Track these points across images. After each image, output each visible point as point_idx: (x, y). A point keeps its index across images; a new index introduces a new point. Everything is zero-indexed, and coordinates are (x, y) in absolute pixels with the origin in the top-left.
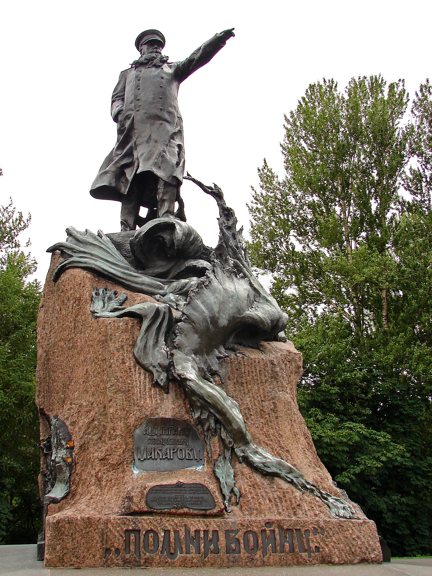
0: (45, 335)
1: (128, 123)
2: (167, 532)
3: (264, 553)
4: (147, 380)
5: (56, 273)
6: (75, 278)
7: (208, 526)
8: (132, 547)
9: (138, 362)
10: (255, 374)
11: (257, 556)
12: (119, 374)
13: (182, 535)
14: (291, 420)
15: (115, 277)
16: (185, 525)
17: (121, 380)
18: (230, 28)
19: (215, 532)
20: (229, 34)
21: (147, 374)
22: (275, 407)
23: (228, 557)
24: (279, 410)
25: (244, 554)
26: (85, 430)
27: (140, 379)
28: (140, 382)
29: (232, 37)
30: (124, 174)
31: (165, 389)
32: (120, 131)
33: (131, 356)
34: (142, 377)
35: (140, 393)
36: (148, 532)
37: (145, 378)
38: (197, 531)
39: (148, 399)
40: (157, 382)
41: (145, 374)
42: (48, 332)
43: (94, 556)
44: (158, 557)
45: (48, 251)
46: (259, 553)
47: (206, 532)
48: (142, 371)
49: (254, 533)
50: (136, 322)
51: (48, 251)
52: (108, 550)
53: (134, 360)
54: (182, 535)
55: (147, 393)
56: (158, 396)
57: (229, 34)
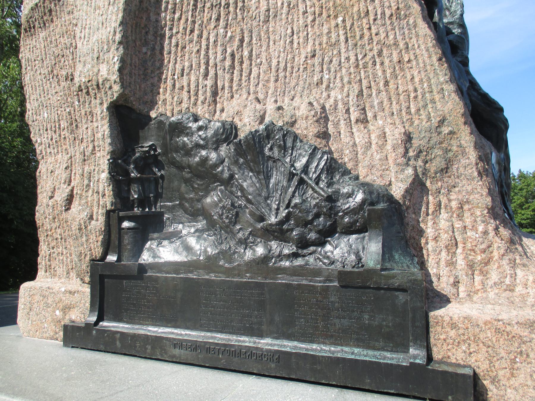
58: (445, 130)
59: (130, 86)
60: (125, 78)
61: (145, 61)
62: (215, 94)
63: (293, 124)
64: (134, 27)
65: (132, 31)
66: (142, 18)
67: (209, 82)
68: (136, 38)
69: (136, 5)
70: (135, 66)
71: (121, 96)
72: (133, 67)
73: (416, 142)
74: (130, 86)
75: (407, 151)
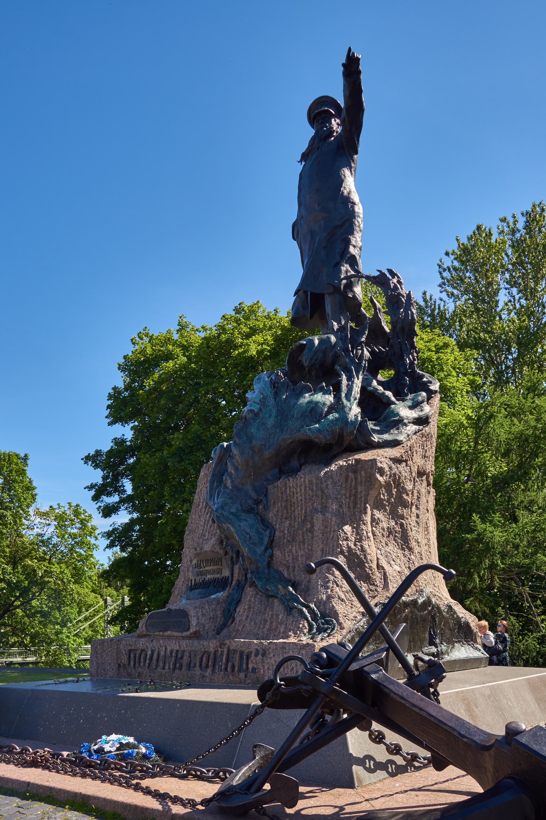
2: (153, 652)
3: (213, 671)
7: (180, 646)
8: (132, 663)
11: (207, 674)
13: (162, 653)
14: (328, 539)
16: (166, 646)
19: (184, 651)
22: (312, 526)
23: (187, 674)
24: (316, 528)
25: (197, 671)
28: (205, 520)
35: (203, 530)
36: (143, 651)
38: (171, 651)
43: (113, 669)
44: (145, 672)
46: (209, 671)
47: (177, 651)
49: (209, 654)
52: (119, 666)
54: (162, 653)
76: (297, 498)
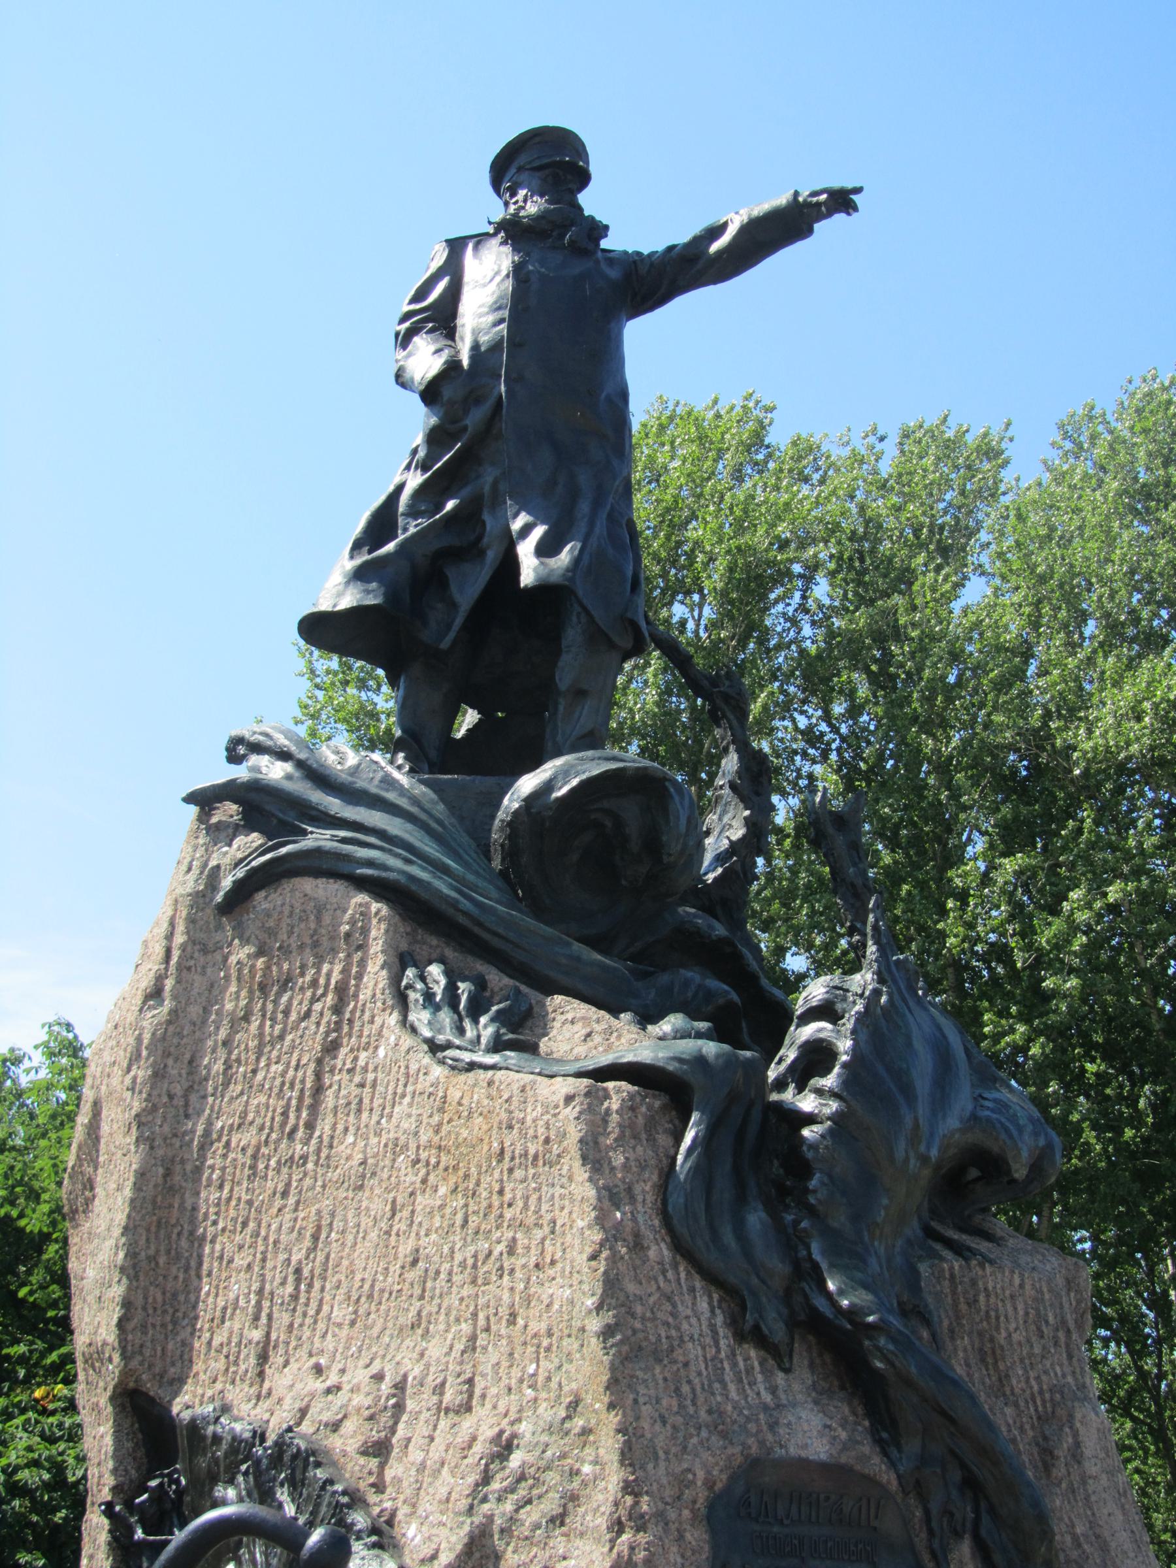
0: (165, 1099)
1: (475, 418)
4: (719, 1319)
5: (239, 885)
6: (320, 910)
9: (680, 1247)
10: (1013, 1326)
12: (631, 1287)
15: (476, 930)
17: (639, 1309)
18: (850, 186)
20: (841, 201)
21: (716, 1296)
26: (477, 1485)
27: (700, 1311)
29: (840, 217)
30: (444, 584)
31: (778, 1356)
32: (436, 439)
33: (657, 1222)
34: (703, 1305)
37: (712, 1311)
39: (732, 1387)
40: (757, 1328)
41: (710, 1297)
42: (178, 1090)
45: (190, 799)
48: (698, 1284)
50: (657, 1104)
51: (190, 799)
53: (668, 1239)
55: (726, 1365)
56: (760, 1378)
57: (841, 201)
58: (579, 1423)
59: (141, 1353)
60: (130, 1337)
61: (175, 1295)
62: (263, 1358)
63: (335, 1426)
64: (153, 1229)
65: (148, 1240)
66: (171, 1206)
67: (257, 1335)
68: (158, 1251)
69: (156, 1186)
70: (155, 1309)
71: (125, 1373)
72: (150, 1311)
73: (516, 1460)
74: (141, 1353)
75: (486, 1479)
76: (1010, 1335)
